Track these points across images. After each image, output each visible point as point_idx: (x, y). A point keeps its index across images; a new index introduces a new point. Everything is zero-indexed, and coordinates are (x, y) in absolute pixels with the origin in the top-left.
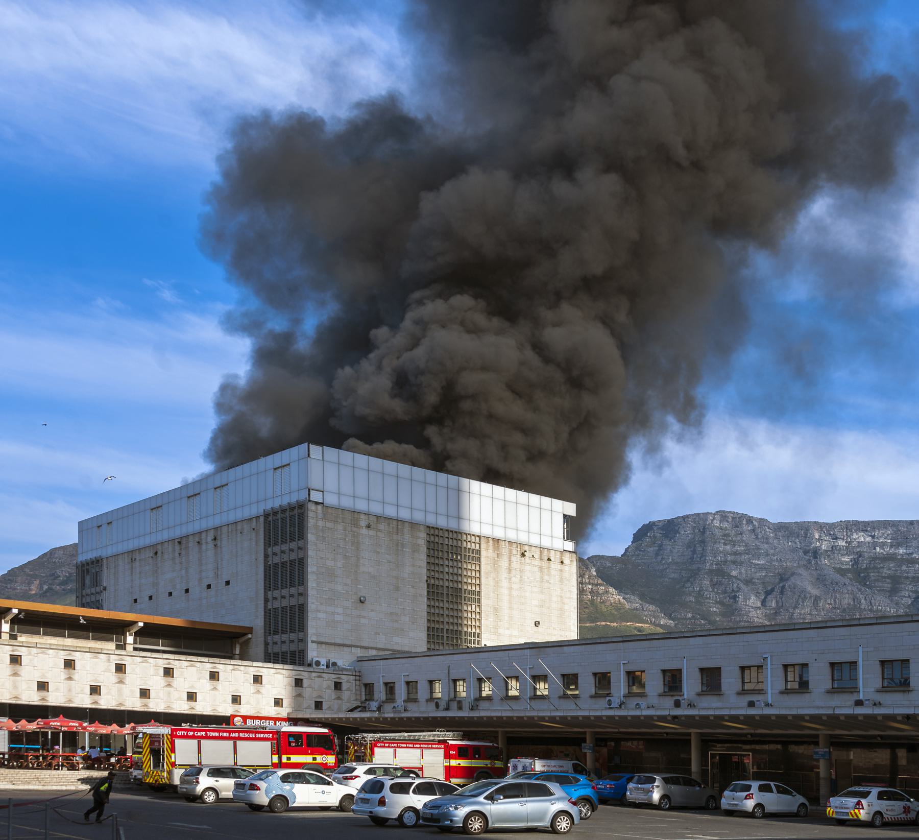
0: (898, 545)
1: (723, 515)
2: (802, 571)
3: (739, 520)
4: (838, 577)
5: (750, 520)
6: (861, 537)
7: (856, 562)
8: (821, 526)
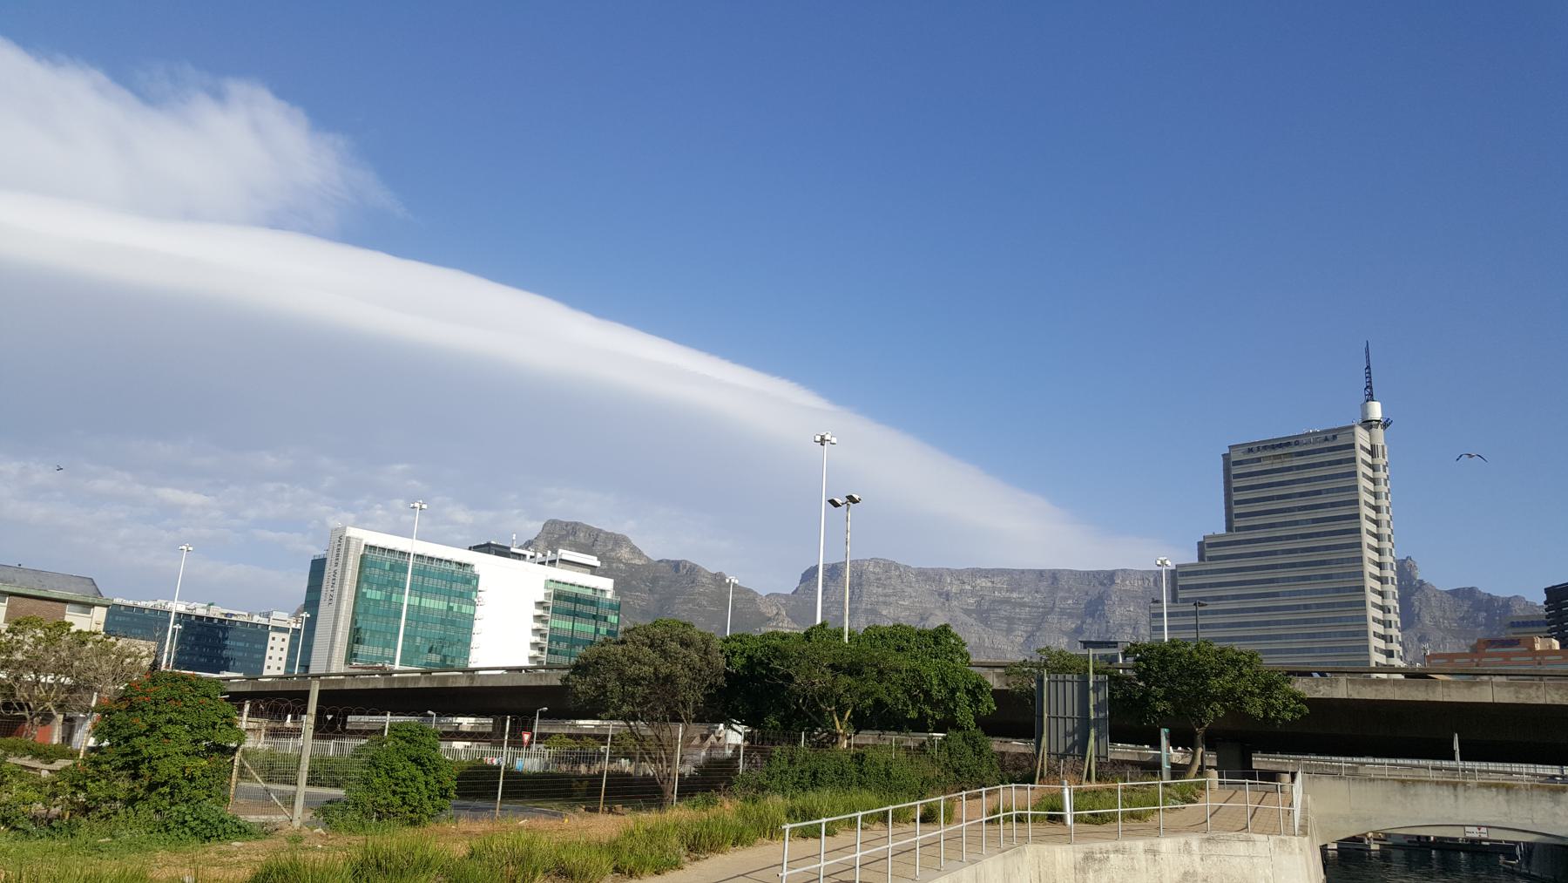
0: (1013, 591)
1: (876, 562)
2: (938, 612)
3: (889, 566)
4: (965, 618)
5: (897, 567)
6: (983, 583)
7: (979, 604)
8: (951, 572)
